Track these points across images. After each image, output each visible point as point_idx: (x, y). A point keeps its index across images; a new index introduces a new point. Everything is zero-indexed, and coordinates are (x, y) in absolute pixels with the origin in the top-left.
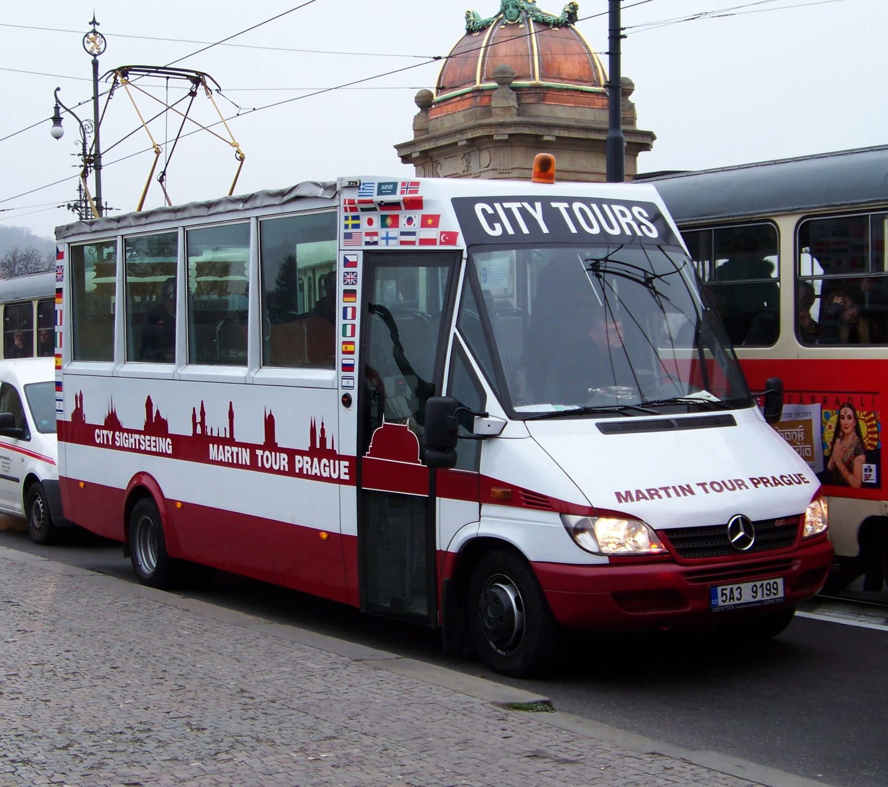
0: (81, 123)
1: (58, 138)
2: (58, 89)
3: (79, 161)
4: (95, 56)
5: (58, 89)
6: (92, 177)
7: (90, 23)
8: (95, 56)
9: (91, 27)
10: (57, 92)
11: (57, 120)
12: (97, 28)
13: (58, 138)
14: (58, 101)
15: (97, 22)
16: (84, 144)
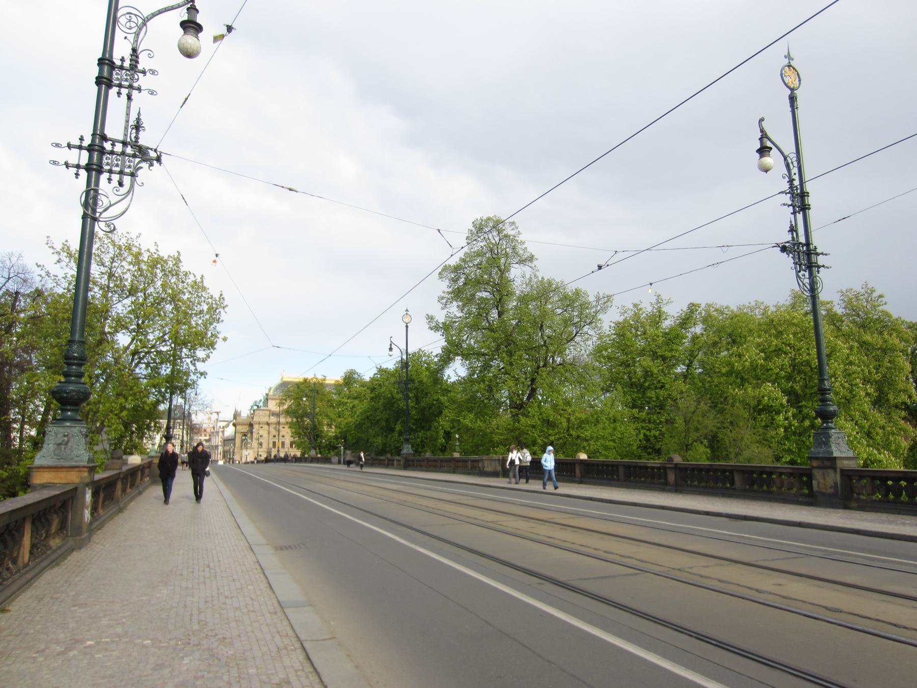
0: (785, 159)
1: (766, 171)
2: (761, 120)
3: (787, 199)
4: (792, 90)
5: (761, 120)
6: (800, 217)
7: (785, 57)
8: (792, 90)
9: (786, 61)
10: (763, 123)
11: (763, 151)
12: (792, 63)
13: (766, 171)
14: (762, 131)
15: (792, 56)
16: (791, 181)
